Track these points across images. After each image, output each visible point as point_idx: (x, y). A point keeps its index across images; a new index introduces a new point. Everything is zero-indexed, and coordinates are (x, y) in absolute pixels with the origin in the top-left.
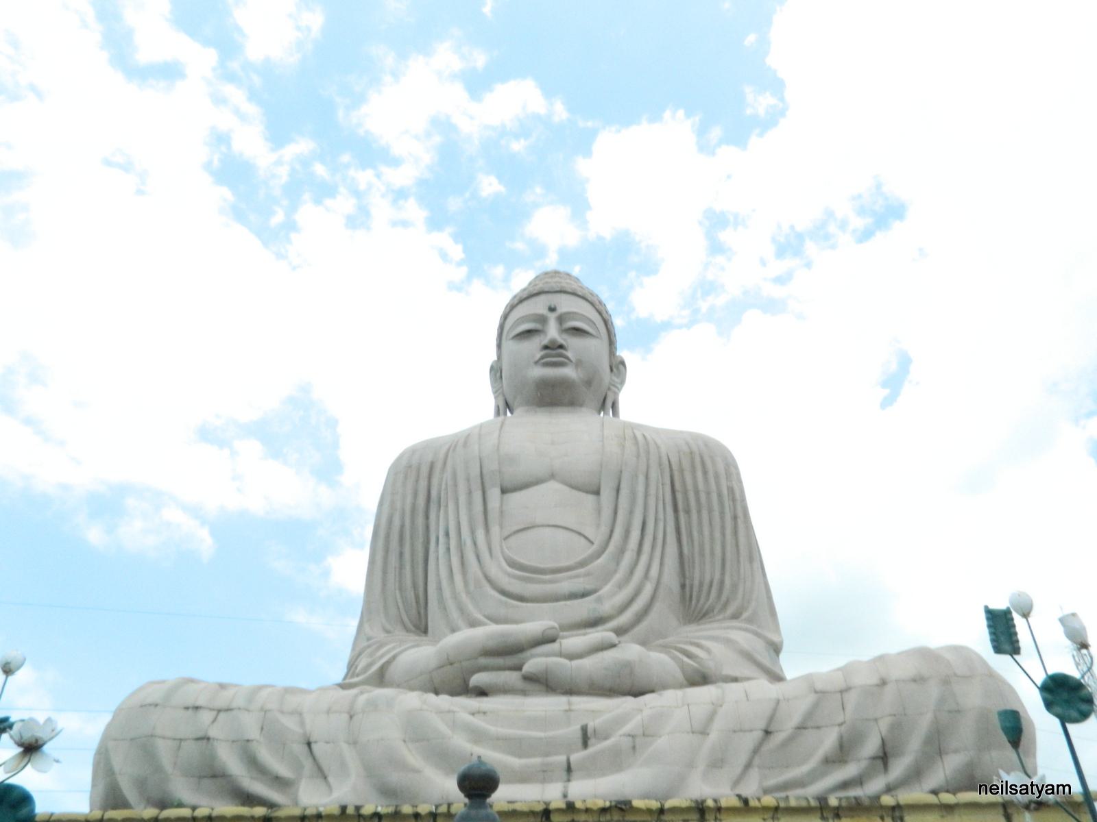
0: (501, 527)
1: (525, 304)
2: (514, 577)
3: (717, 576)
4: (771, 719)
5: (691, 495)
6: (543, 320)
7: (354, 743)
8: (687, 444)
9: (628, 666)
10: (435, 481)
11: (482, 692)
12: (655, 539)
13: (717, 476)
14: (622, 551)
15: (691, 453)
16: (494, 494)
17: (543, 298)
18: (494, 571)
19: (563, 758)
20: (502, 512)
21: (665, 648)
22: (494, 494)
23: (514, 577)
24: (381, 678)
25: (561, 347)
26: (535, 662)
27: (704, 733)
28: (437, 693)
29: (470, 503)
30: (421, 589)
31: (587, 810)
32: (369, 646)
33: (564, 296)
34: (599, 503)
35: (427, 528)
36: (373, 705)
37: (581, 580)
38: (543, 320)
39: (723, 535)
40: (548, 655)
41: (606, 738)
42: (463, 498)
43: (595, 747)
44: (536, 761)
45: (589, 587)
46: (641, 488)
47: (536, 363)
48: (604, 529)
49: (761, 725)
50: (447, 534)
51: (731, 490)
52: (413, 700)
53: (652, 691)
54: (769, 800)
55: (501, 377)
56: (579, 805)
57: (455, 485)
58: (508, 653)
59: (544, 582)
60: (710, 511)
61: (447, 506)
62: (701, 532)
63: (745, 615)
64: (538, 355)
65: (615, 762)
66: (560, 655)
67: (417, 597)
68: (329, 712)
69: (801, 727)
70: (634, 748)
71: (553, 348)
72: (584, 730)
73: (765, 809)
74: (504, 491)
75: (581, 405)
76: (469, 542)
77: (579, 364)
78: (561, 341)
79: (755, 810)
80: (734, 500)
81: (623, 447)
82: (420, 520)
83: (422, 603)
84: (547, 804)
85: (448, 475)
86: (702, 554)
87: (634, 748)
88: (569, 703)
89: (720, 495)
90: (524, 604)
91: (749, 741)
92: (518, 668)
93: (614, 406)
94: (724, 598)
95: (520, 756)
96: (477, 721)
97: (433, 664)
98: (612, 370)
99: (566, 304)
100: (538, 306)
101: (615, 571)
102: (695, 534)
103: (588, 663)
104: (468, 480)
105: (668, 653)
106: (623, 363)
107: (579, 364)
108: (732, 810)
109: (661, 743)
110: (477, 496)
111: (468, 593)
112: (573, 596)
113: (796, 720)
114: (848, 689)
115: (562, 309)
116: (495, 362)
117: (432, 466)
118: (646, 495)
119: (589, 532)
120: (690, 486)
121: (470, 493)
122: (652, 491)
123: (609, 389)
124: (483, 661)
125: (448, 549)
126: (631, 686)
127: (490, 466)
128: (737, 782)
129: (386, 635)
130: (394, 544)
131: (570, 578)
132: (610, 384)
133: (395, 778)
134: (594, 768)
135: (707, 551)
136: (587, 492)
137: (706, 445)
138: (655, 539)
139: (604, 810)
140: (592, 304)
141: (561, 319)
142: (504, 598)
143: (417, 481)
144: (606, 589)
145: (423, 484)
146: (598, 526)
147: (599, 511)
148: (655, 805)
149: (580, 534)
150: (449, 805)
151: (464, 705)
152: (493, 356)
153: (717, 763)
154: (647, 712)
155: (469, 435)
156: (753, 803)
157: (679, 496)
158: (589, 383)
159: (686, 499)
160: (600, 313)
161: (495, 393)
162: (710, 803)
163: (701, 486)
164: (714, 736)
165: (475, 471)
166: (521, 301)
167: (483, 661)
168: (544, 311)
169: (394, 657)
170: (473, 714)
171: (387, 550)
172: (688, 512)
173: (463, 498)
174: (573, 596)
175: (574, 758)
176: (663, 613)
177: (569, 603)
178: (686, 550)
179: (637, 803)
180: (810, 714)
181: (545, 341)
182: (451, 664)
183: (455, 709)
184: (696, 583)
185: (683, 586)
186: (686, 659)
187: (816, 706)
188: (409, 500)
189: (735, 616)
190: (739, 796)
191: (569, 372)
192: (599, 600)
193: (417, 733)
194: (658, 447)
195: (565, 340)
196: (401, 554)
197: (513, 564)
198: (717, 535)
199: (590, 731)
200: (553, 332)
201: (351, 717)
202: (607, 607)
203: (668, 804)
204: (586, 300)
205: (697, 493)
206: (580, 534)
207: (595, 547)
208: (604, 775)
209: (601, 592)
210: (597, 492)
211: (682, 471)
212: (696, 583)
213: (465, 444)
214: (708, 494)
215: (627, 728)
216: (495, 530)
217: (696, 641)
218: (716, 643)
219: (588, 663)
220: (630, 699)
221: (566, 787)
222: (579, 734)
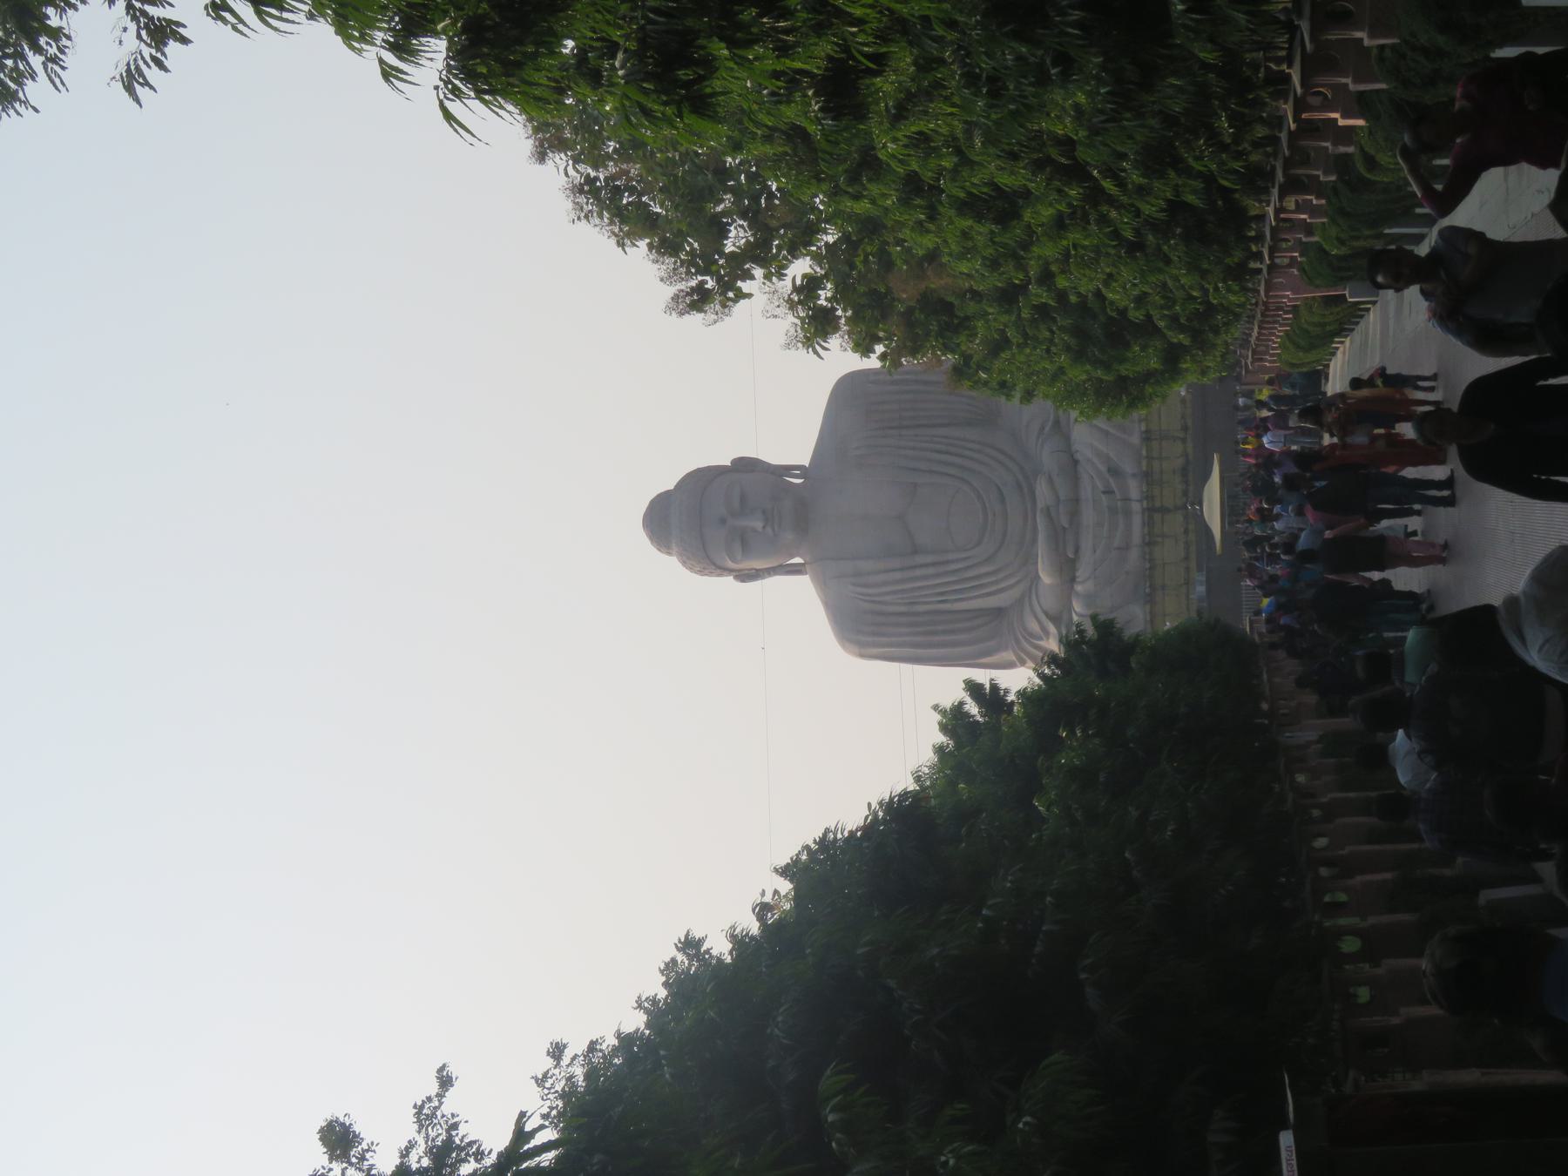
10: (891, 609)
11: (1077, 550)
22: (920, 559)
25: (764, 512)
26: (1065, 522)
27: (1107, 433)
28: (1073, 580)
50: (942, 594)
64: (769, 530)
74: (916, 551)
84: (1144, 510)
85: (888, 598)
93: (788, 470)
104: (902, 581)
110: (918, 572)
112: (1002, 500)
116: (736, 578)
118: (914, 448)
125: (955, 591)
148: (1144, 463)
152: (730, 579)
164: (1111, 430)
165: (898, 575)
169: (1046, 613)
174: (1002, 500)
181: (759, 525)
196: (944, 632)
197: (979, 543)
213: (866, 586)
216: (951, 556)
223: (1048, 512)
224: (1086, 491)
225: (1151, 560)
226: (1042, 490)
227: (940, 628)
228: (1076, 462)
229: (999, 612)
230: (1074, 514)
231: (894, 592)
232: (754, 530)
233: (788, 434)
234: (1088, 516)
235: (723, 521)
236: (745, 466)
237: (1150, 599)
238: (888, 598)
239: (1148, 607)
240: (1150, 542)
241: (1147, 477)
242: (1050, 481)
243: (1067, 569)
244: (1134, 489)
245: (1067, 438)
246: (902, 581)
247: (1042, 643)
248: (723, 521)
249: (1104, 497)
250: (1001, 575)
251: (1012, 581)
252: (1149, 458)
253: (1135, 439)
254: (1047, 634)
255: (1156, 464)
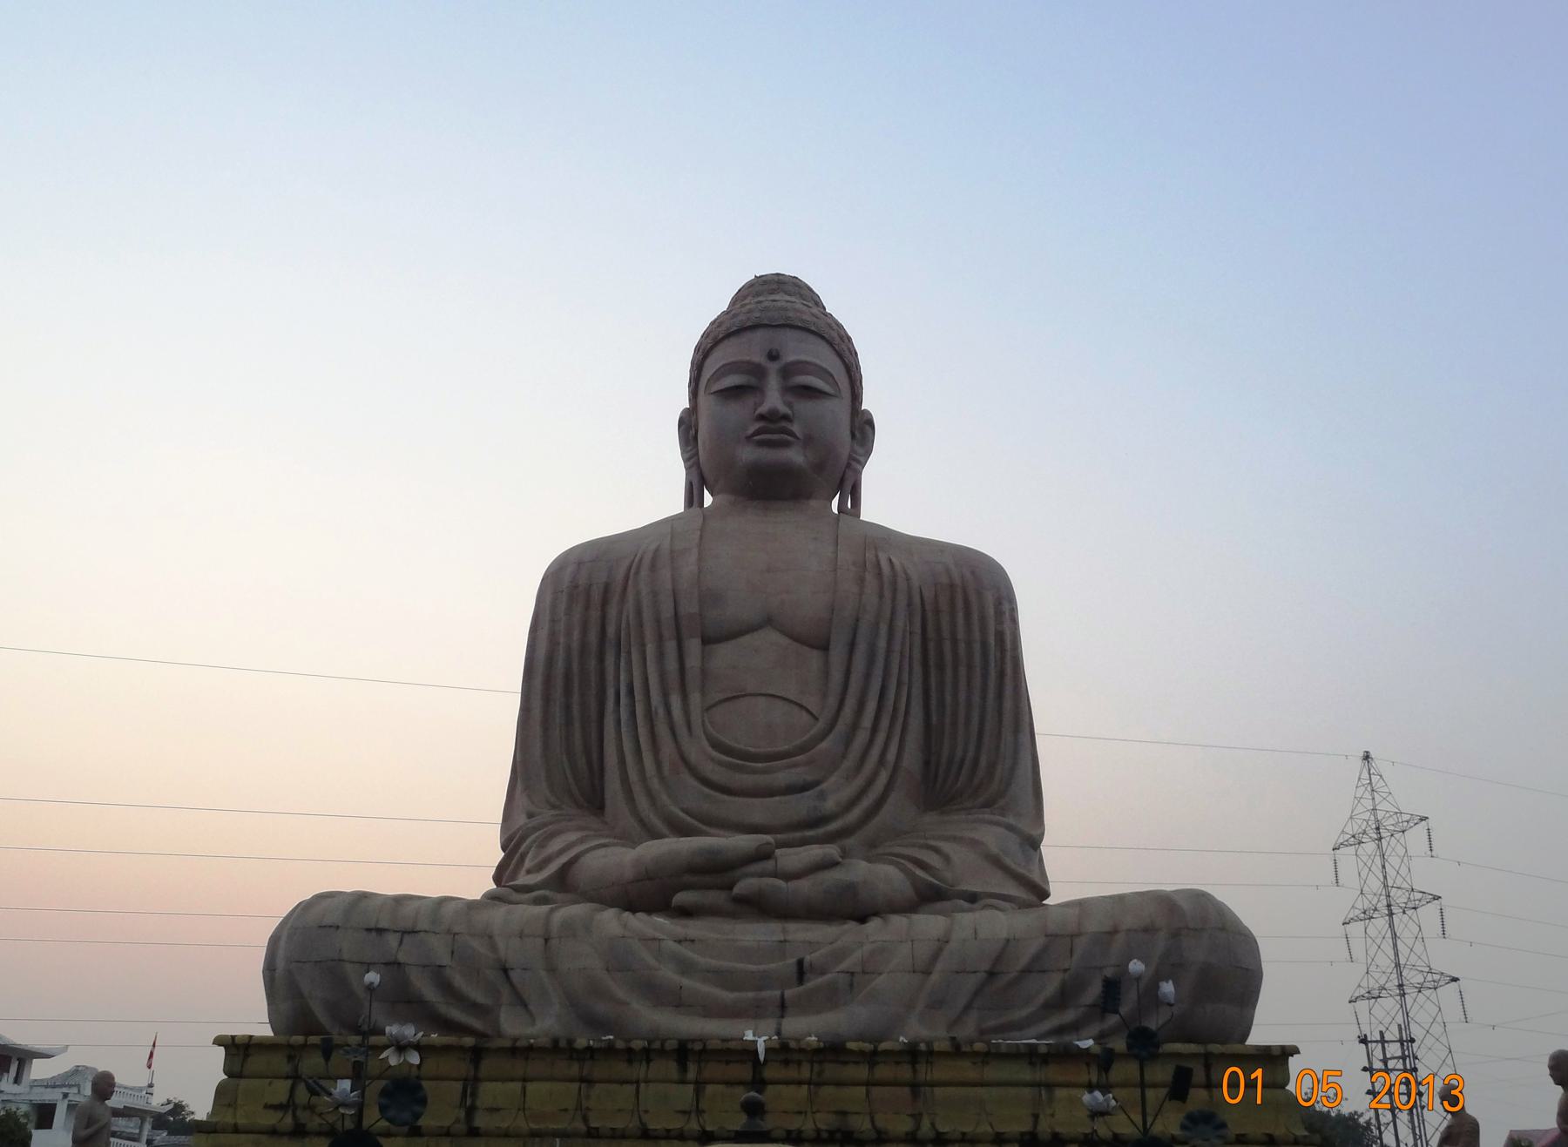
0: (703, 694)
1: (734, 340)
2: (720, 763)
3: (971, 754)
4: (999, 959)
5: (947, 646)
6: (758, 371)
7: (552, 970)
8: (948, 570)
9: (850, 889)
10: (612, 612)
11: (686, 913)
12: (895, 709)
13: (983, 619)
14: (855, 726)
15: (952, 586)
16: (693, 646)
17: (759, 335)
18: (693, 756)
19: (778, 993)
20: (704, 672)
21: (893, 858)
22: (693, 646)
23: (720, 763)
24: (563, 882)
25: (786, 418)
26: (747, 885)
27: (927, 972)
28: (633, 909)
29: (661, 656)
30: (595, 756)
31: (801, 1050)
32: (536, 829)
33: (790, 333)
34: (827, 663)
35: (602, 674)
36: (569, 928)
37: (798, 770)
38: (758, 371)
39: (984, 698)
40: (761, 875)
41: (823, 973)
42: (650, 649)
43: (813, 982)
44: (750, 995)
45: (809, 778)
46: (882, 644)
47: (749, 438)
48: (832, 701)
49: (986, 966)
51: (1000, 636)
52: (610, 921)
53: (876, 914)
54: (979, 1046)
55: (695, 438)
56: (793, 1044)
57: (641, 625)
58: (716, 870)
59: (754, 772)
60: (970, 667)
61: (629, 653)
62: (955, 694)
63: (1001, 802)
64: (757, 425)
65: (831, 998)
66: (775, 875)
67: (589, 763)
68: (521, 936)
69: (1027, 971)
70: (851, 985)
71: (771, 419)
72: (800, 963)
73: (976, 1054)
74: (706, 641)
75: (809, 497)
76: (661, 711)
77: (808, 441)
78: (783, 409)
79: (965, 1053)
80: (1003, 651)
81: (861, 581)
82: (592, 663)
83: (597, 771)
85: (630, 605)
86: (954, 724)
87: (851, 985)
88: (784, 931)
89: (984, 644)
90: (725, 797)
91: (971, 982)
92: (731, 888)
94: (976, 781)
95: (732, 989)
96: (686, 951)
97: (629, 874)
98: (853, 436)
99: (797, 349)
100: (751, 349)
101: (844, 756)
102: (948, 698)
103: (804, 886)
104: (658, 621)
105: (897, 865)
106: (870, 423)
107: (808, 441)
108: (943, 1054)
109: (880, 981)
110: (671, 646)
111: (662, 778)
113: (1023, 962)
114: (1079, 935)
115: (791, 358)
116: (686, 411)
117: (607, 589)
118: (889, 651)
119: (812, 702)
120: (946, 634)
121: (660, 639)
122: (897, 647)
123: (848, 466)
124: (688, 878)
125: (633, 714)
126: (854, 908)
127: (689, 607)
128: (953, 1024)
129: (553, 812)
130: (558, 693)
131: (789, 767)
132: (851, 458)
133: (601, 1008)
134: (808, 1005)
135: (961, 719)
136: (812, 646)
137: (973, 573)
138: (895, 709)
139: (817, 1051)
140: (830, 344)
141: (787, 372)
142: (707, 790)
143: (587, 608)
144: (833, 779)
145: (595, 614)
146: (824, 696)
147: (826, 674)
148: (868, 1047)
149: (801, 706)
150: (663, 1042)
151: (661, 923)
152: (685, 403)
153: (936, 1004)
154: (868, 947)
155: (657, 550)
156: (964, 1049)
157: (931, 645)
158: (819, 467)
159: (940, 653)
160: (840, 356)
161: (685, 461)
162: (923, 1047)
163: (961, 635)
164: (935, 977)
165: (667, 612)
166: (728, 336)
167: (688, 878)
168: (758, 358)
170: (680, 942)
171: (547, 699)
172: (941, 667)
173: (650, 649)
175: (788, 993)
176: (899, 808)
177: (788, 798)
178: (934, 719)
179: (851, 1045)
180: (1037, 958)
181: (763, 409)
182: (650, 879)
183: (658, 935)
184: (944, 760)
185: (927, 763)
186: (919, 873)
187: (1045, 950)
188: (576, 634)
189: (988, 805)
190: (953, 1039)
191: (795, 456)
192: (822, 796)
193: (618, 960)
194: (908, 579)
195: (789, 405)
196: (567, 708)
198: (976, 699)
199: (806, 964)
200: (773, 399)
201: (546, 940)
202: (830, 805)
203: (883, 1046)
204: (823, 338)
205: (955, 641)
206: (801, 706)
207: (821, 725)
208: (819, 1012)
209: (824, 786)
210: (824, 647)
211: (937, 611)
212: (944, 760)
213: (653, 567)
214: (969, 643)
215: (843, 966)
216: (695, 698)
217: (932, 843)
218: (961, 847)
219: (804, 886)
220: (851, 925)
221: (780, 1024)
222: (794, 969)
223: (763, 855)
224: (801, 933)
225: (647, 1055)
226: (815, 852)
227: (576, 698)
228: (862, 920)
229: (593, 801)
230: (759, 907)
231: (639, 612)
232: (761, 404)
233: (908, 491)
234: (755, 933)
235: (773, 356)
236: (862, 429)
237: (559, 1049)
238: (630, 605)
239: (544, 1041)
240: (685, 1052)
241: (833, 1050)
242: (828, 865)
243: (650, 894)
244: (807, 1028)
245: (910, 908)
246: (658, 621)
247: (528, 864)
248: (773, 356)
249: (794, 960)
250: (655, 784)
251: (643, 802)
252: (873, 1058)
253: (914, 1030)
254: (539, 867)
255: (862, 1072)
